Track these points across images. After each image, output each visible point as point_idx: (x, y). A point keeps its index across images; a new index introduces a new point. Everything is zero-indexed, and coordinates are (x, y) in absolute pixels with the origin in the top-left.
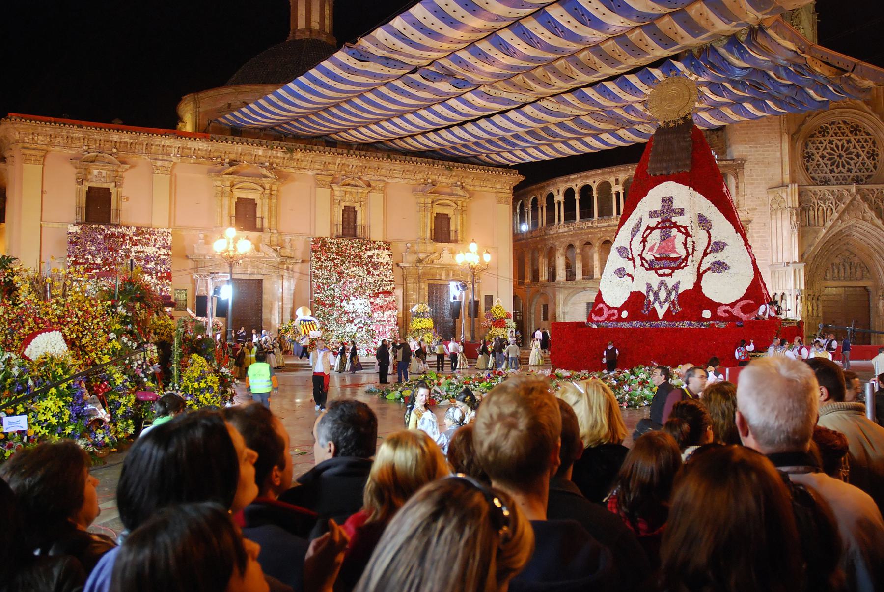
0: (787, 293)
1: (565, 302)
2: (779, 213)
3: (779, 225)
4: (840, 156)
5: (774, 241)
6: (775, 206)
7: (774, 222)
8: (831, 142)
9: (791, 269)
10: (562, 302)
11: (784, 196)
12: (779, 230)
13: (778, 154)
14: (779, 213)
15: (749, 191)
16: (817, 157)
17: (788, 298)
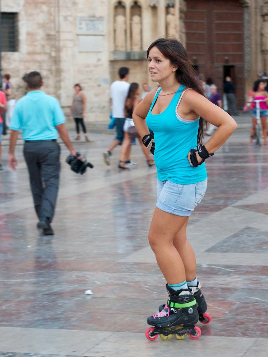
17: (147, 15)
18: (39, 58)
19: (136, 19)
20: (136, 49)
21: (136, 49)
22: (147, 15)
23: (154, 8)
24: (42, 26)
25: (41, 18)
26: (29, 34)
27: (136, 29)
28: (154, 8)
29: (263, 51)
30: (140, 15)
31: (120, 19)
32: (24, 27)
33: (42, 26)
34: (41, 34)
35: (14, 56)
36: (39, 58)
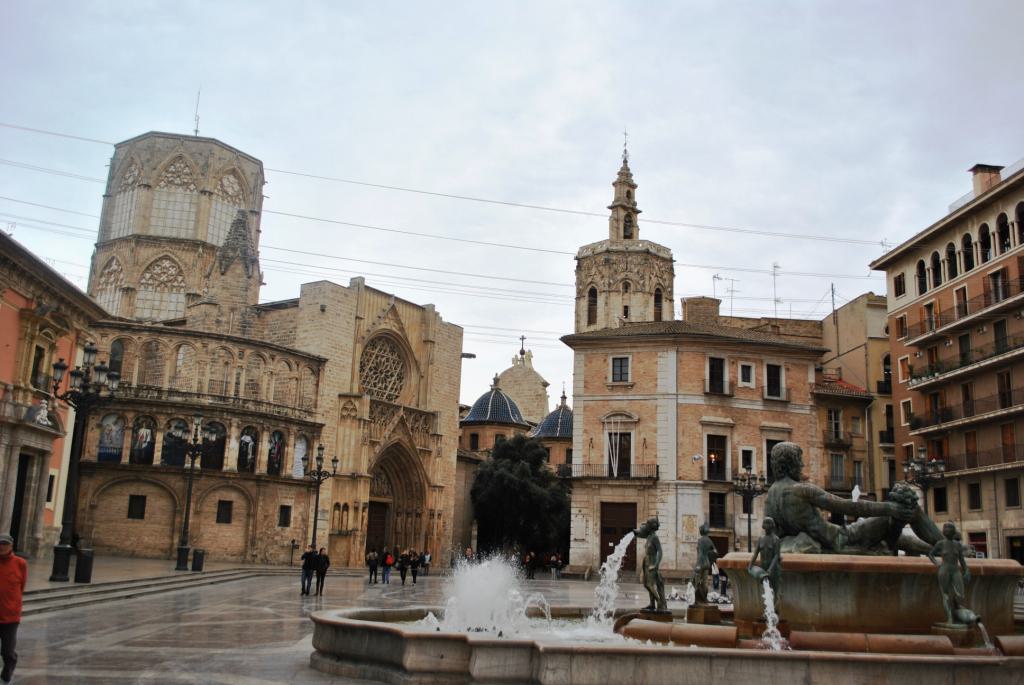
0: (351, 505)
1: (102, 492)
2: (349, 421)
3: (347, 432)
4: (381, 373)
5: (340, 449)
6: (345, 413)
7: (341, 429)
8: (377, 357)
9: (362, 480)
10: (91, 492)
11: (357, 404)
12: (347, 438)
13: (350, 361)
14: (349, 421)
15: (326, 392)
16: (367, 370)
17: (351, 513)
18: (298, 530)
19: (345, 513)
20: (344, 529)
21: (344, 529)
22: (351, 513)
23: (356, 509)
24: (301, 514)
25: (301, 509)
26: (295, 518)
27: (345, 518)
28: (356, 509)
29: (396, 533)
30: (347, 511)
31: (337, 512)
32: (293, 514)
33: (301, 514)
34: (300, 517)
35: (288, 529)
36: (298, 530)
